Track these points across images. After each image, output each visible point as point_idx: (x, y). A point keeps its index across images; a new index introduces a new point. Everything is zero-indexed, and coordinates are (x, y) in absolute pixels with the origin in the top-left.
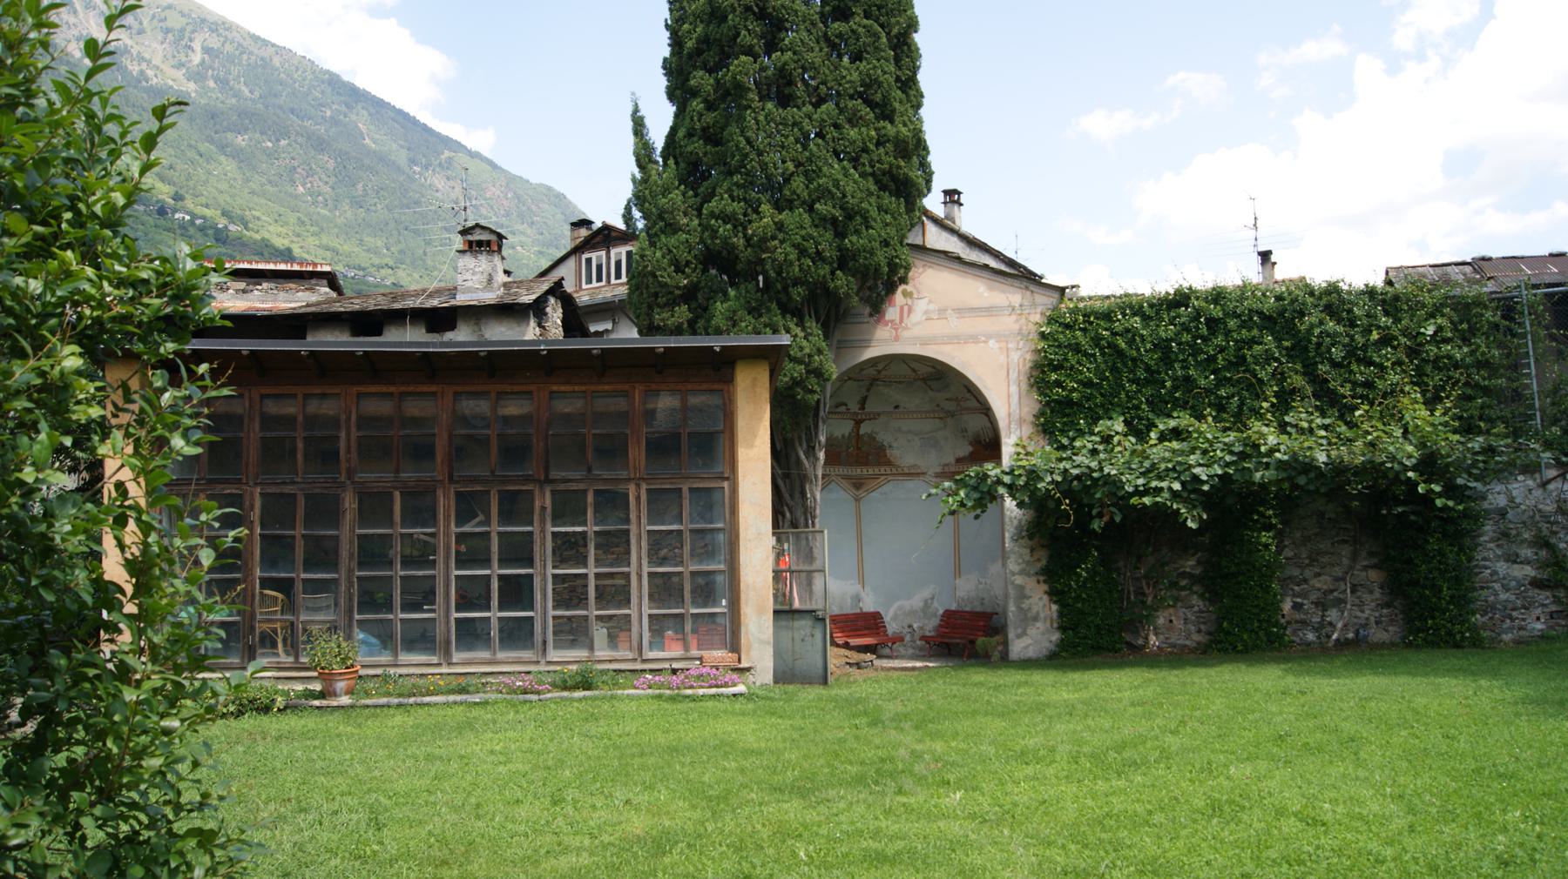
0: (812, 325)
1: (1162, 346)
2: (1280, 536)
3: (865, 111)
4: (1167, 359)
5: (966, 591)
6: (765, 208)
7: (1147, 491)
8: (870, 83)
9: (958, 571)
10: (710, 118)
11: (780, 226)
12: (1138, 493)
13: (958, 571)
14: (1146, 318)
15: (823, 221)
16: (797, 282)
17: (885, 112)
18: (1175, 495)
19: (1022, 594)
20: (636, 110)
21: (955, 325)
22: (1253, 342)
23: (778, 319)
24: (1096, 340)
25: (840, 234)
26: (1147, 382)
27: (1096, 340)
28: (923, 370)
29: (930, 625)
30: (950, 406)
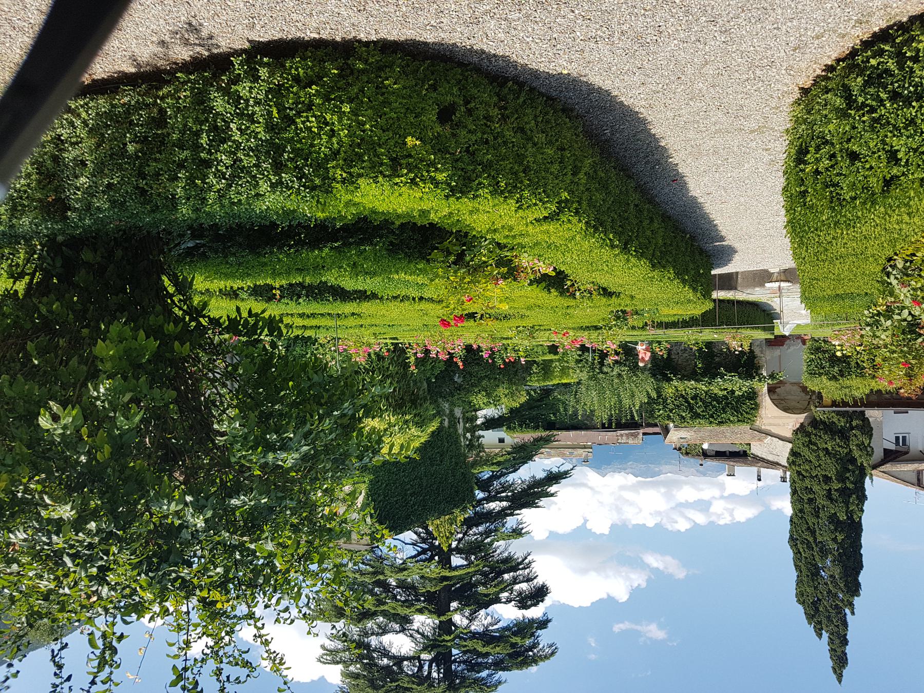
0: (818, 419)
1: (725, 412)
2: (696, 365)
3: (804, 473)
4: (723, 409)
5: (777, 351)
6: (830, 449)
7: (732, 376)
8: (802, 480)
9: (780, 356)
10: (848, 475)
11: (826, 443)
12: (735, 376)
13: (780, 356)
14: (729, 420)
15: (815, 444)
16: (822, 429)
17: (799, 473)
18: (726, 375)
19: (762, 352)
20: (872, 482)
21: (781, 422)
22: (702, 412)
23: (826, 420)
24: (742, 415)
25: (810, 441)
26: (729, 403)
27: (742, 415)
28: (790, 411)
29: (787, 342)
30: (783, 402)
